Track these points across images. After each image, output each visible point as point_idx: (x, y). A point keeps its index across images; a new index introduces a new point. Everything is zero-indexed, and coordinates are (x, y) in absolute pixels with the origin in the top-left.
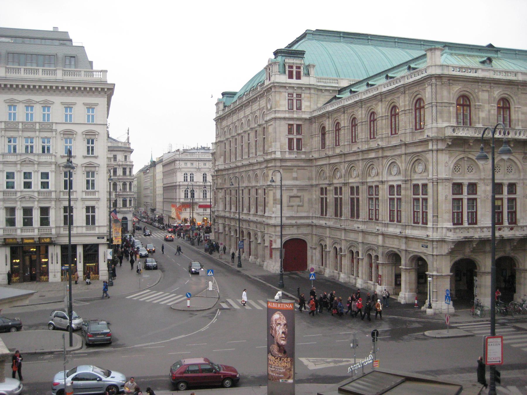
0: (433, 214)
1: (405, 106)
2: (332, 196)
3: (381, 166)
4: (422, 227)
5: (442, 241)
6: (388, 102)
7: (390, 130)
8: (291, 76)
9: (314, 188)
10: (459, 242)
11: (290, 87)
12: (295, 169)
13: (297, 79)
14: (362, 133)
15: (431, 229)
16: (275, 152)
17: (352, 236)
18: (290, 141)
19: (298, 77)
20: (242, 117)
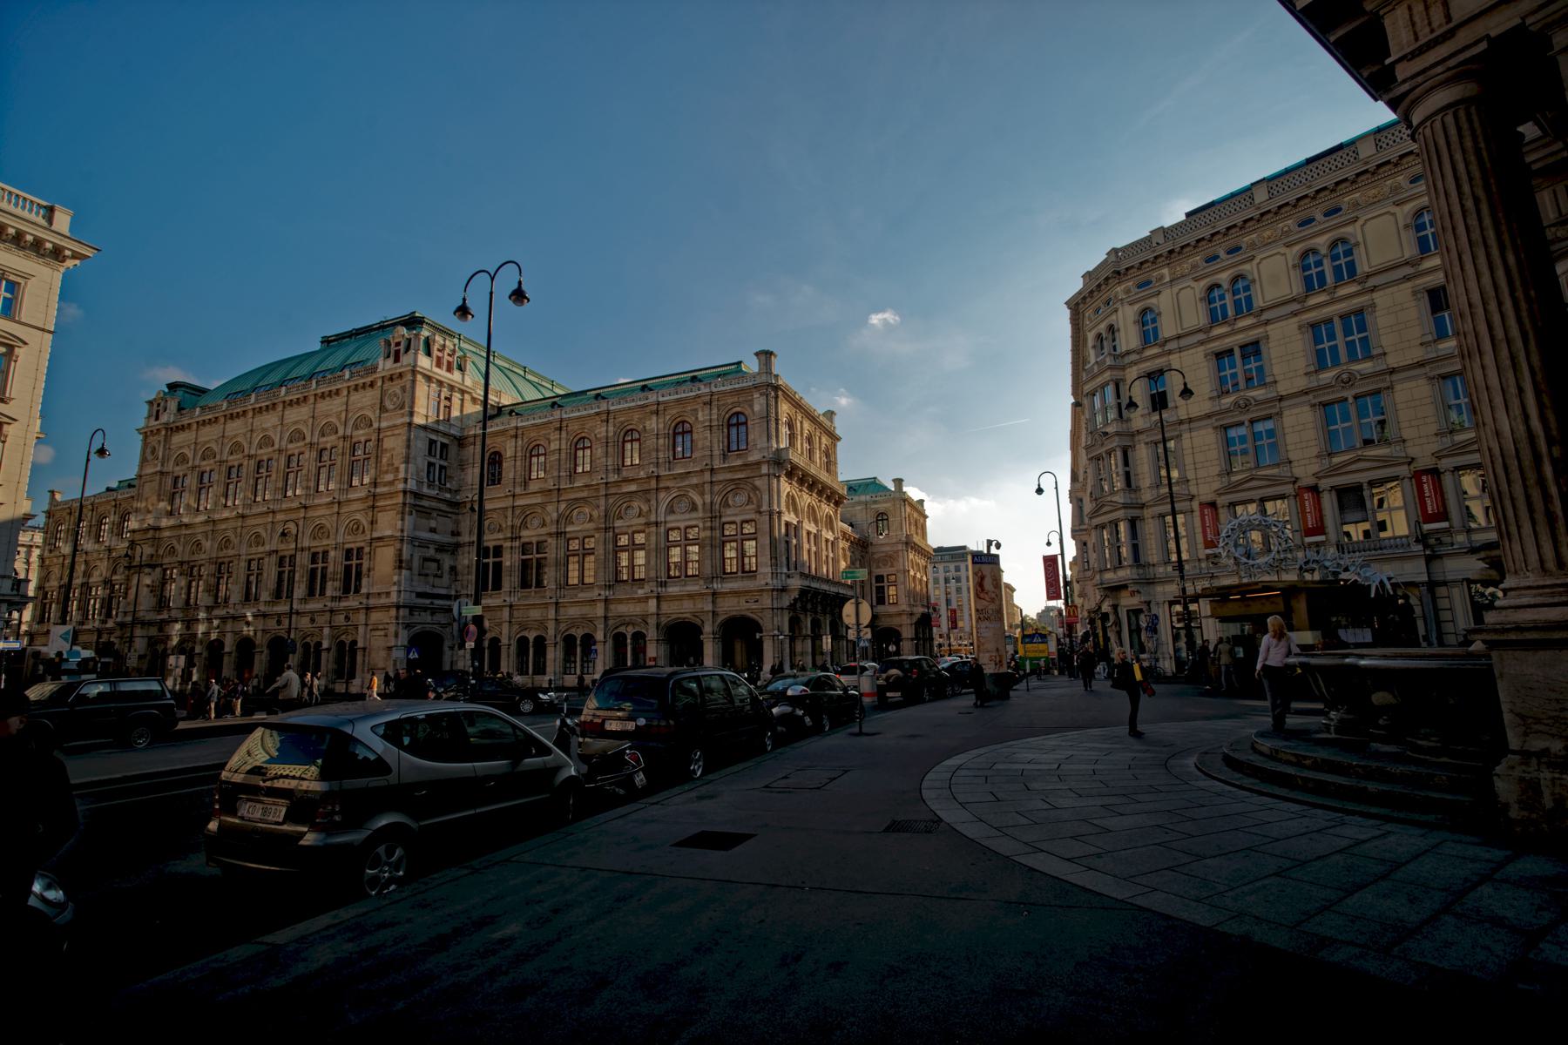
1: (711, 420)
2: (517, 556)
3: (653, 502)
5: (784, 590)
6: (668, 417)
7: (671, 453)
9: (466, 549)
11: (438, 380)
12: (434, 514)
14: (607, 457)
16: (406, 481)
17: (573, 612)
18: (430, 465)
19: (449, 369)
20: (269, 425)
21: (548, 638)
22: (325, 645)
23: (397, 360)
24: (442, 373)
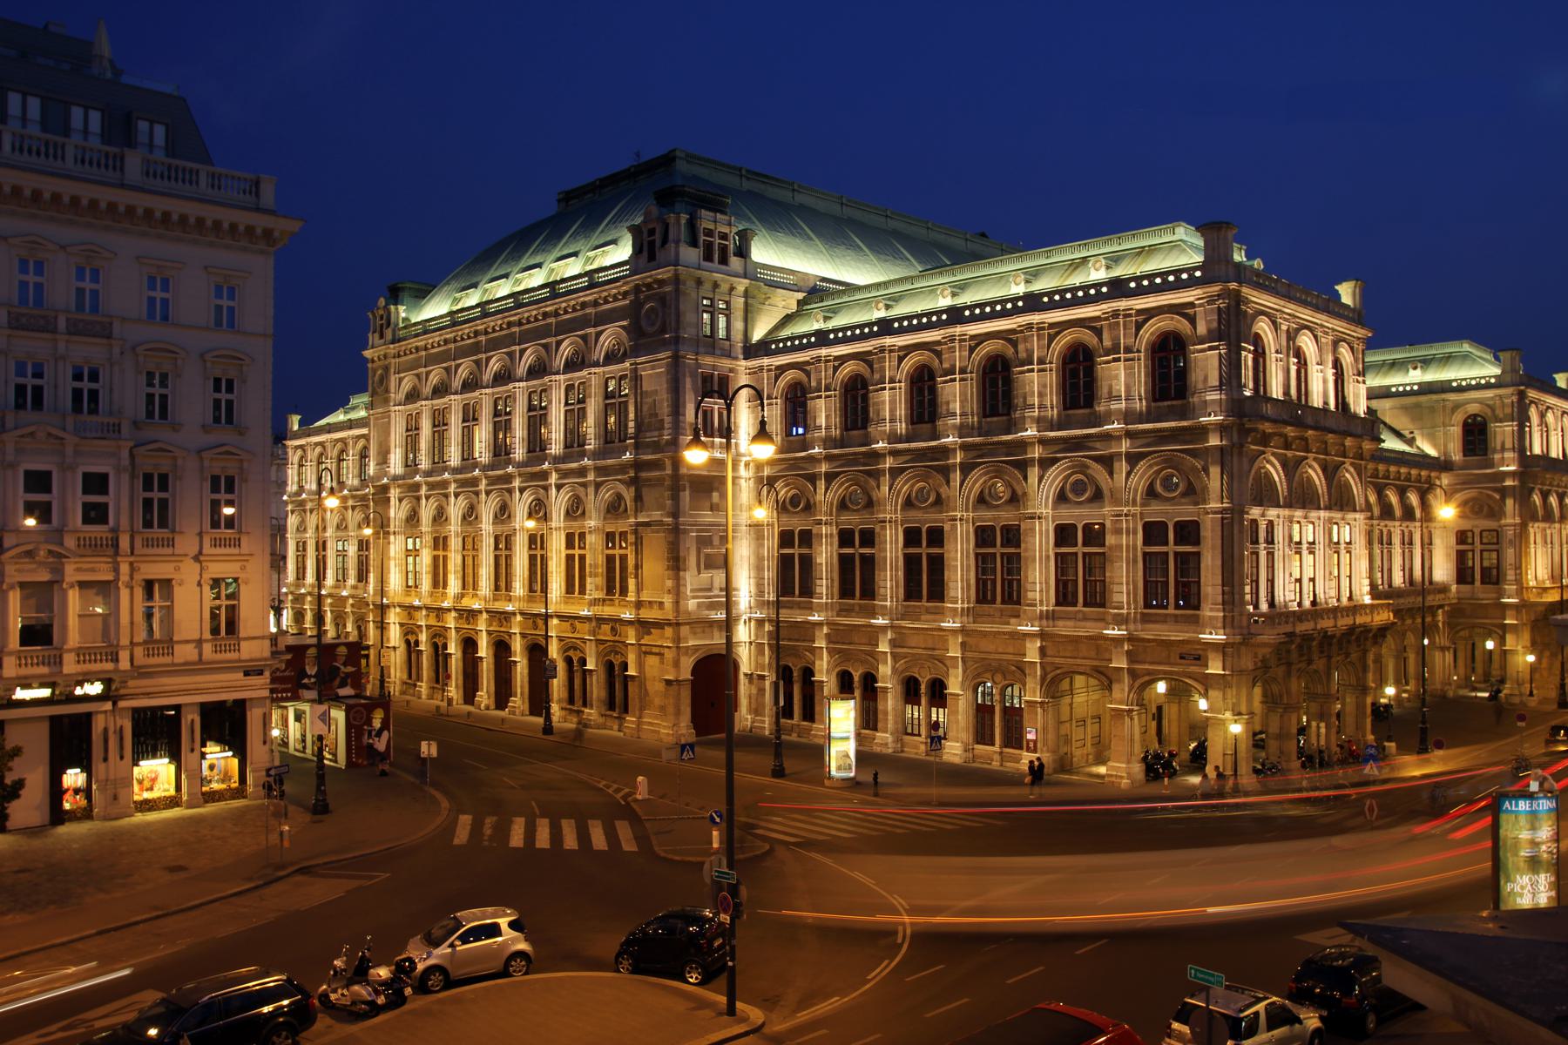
0: (1223, 585)
4: (1176, 616)
8: (708, 257)
10: (1280, 643)
13: (720, 263)
15: (1221, 620)
21: (879, 677)
22: (590, 666)
23: (652, 257)
24: (715, 265)
